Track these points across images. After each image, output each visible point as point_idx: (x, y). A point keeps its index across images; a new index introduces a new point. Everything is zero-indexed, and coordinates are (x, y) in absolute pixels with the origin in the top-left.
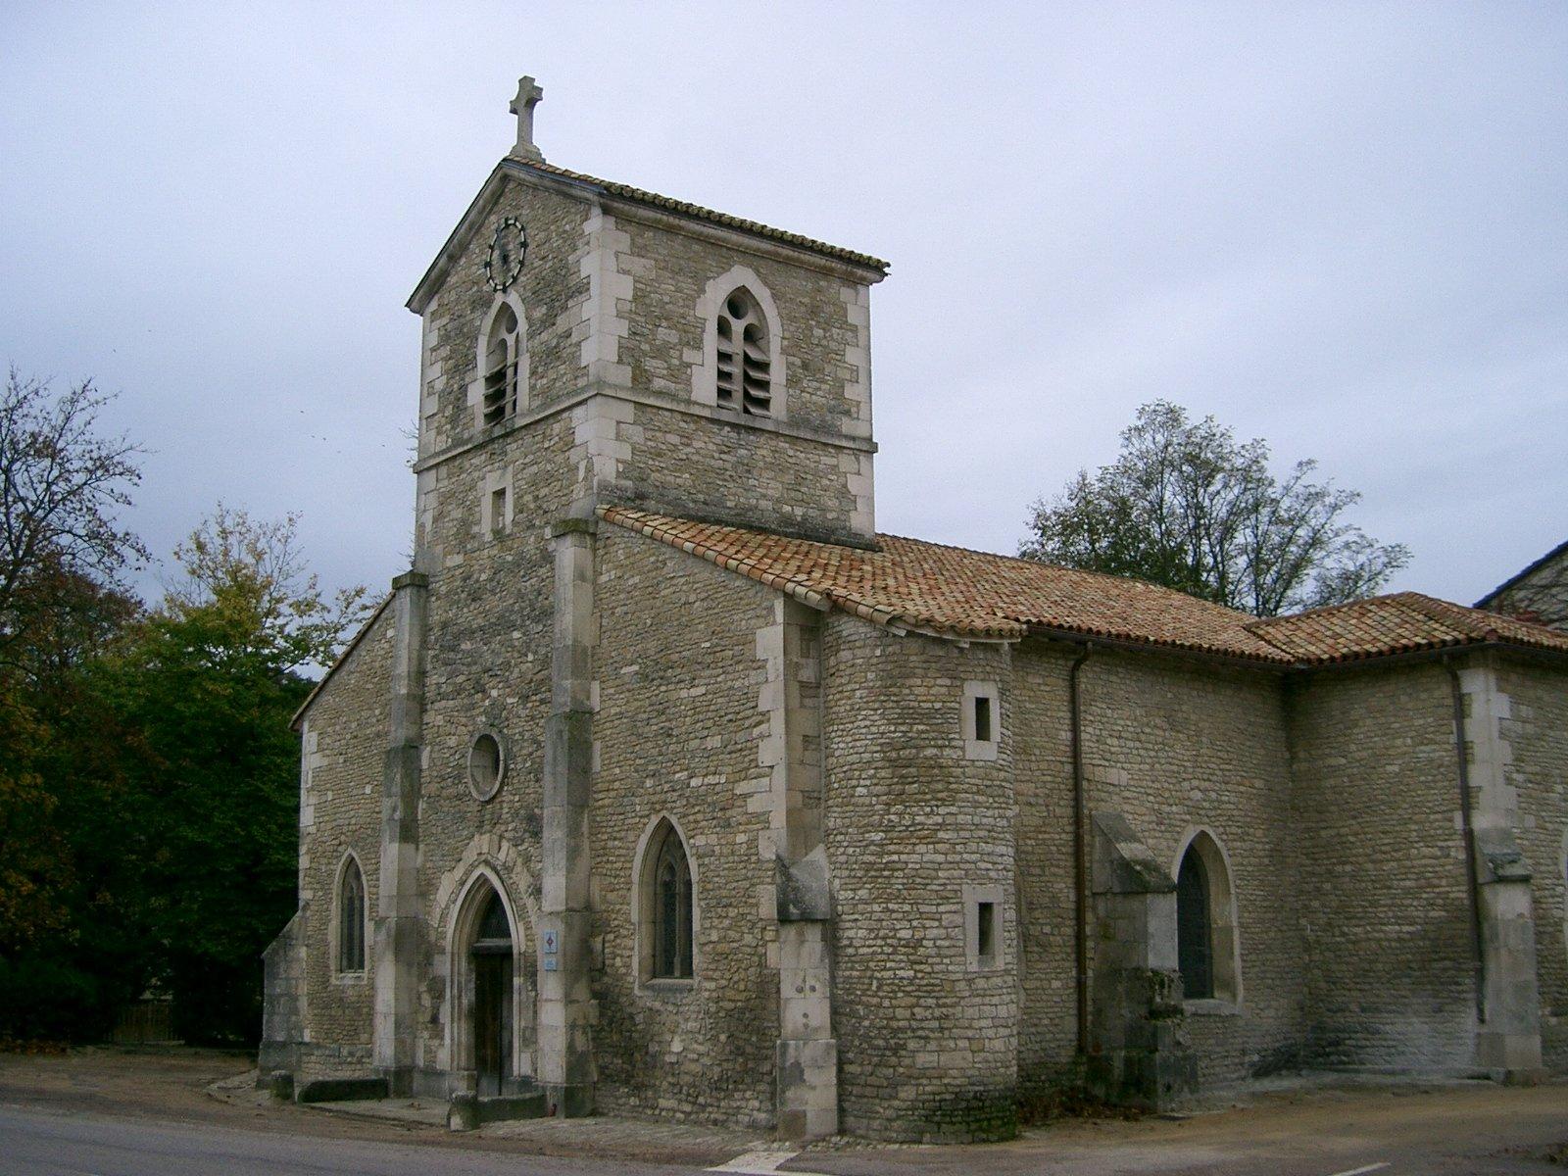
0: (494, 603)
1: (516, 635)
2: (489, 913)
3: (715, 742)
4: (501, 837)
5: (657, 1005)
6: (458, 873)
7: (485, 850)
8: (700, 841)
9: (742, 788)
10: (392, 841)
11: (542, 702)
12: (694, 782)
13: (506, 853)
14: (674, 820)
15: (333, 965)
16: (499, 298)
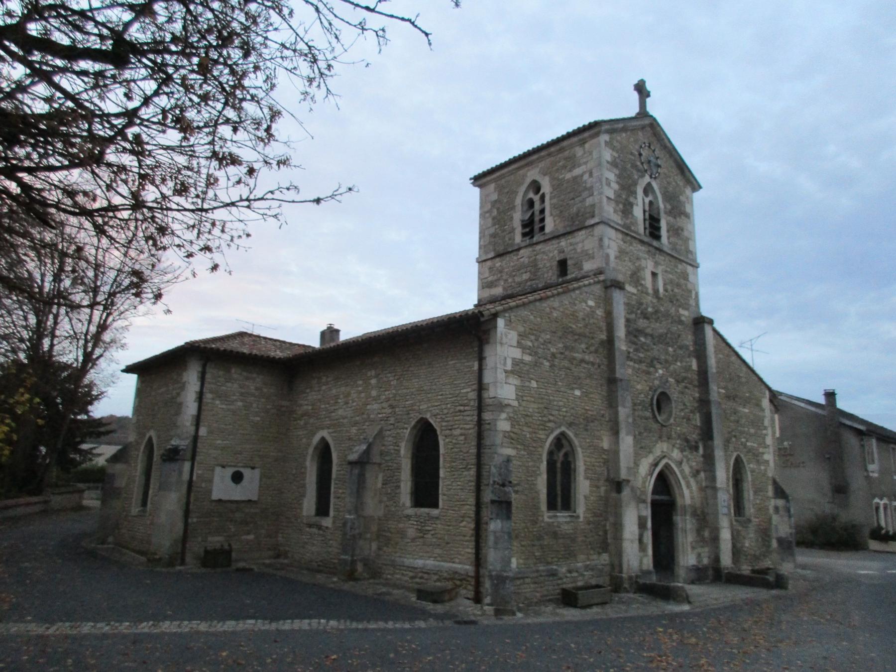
0: (659, 328)
1: (670, 349)
2: (664, 483)
3: (752, 431)
4: (674, 446)
5: (740, 528)
6: (651, 459)
7: (665, 450)
8: (751, 466)
9: (761, 450)
10: (627, 434)
11: (686, 387)
12: (748, 444)
13: (676, 454)
14: (742, 456)
15: (544, 506)
16: (647, 179)
